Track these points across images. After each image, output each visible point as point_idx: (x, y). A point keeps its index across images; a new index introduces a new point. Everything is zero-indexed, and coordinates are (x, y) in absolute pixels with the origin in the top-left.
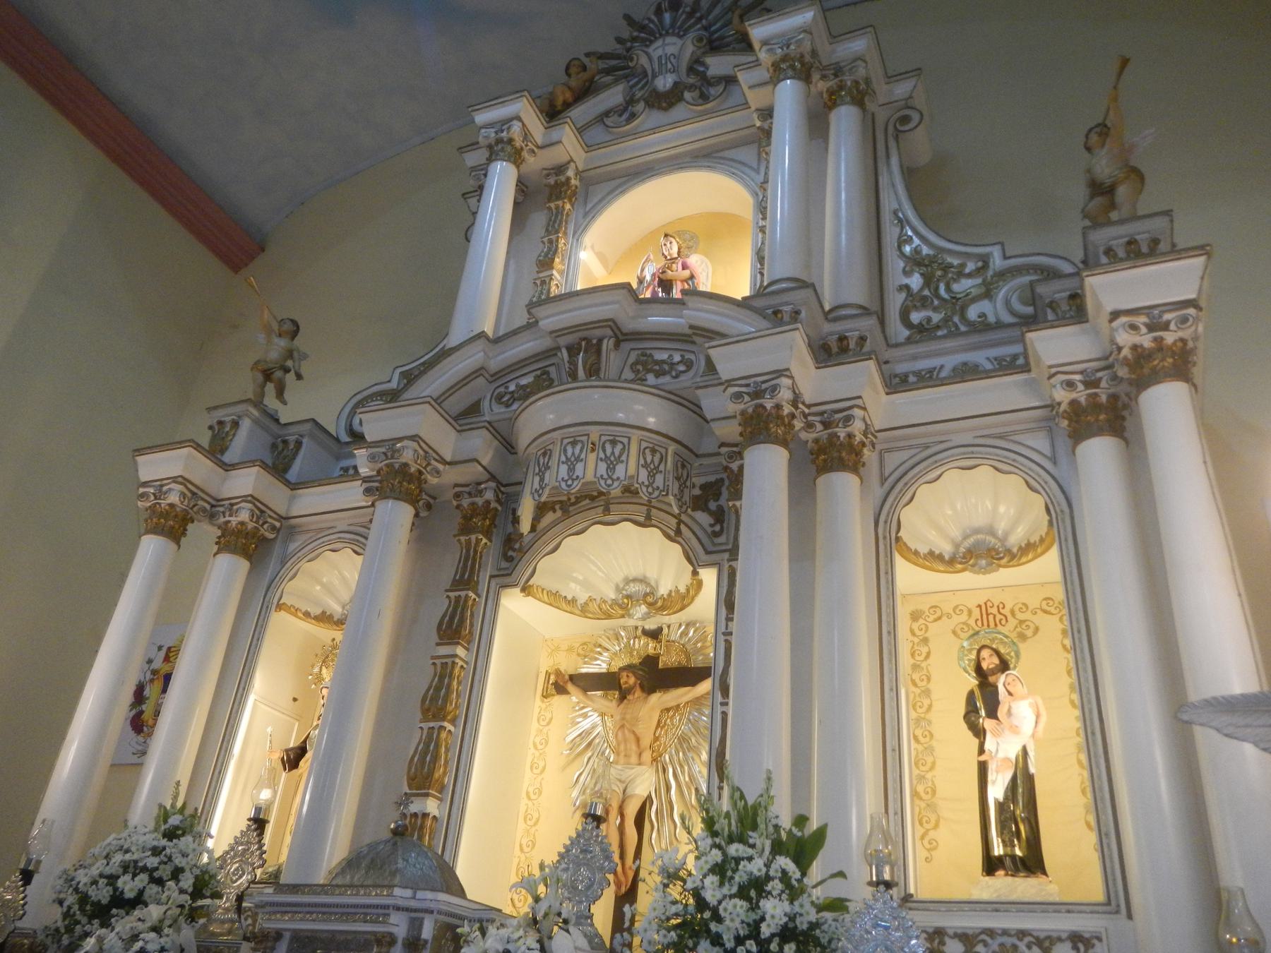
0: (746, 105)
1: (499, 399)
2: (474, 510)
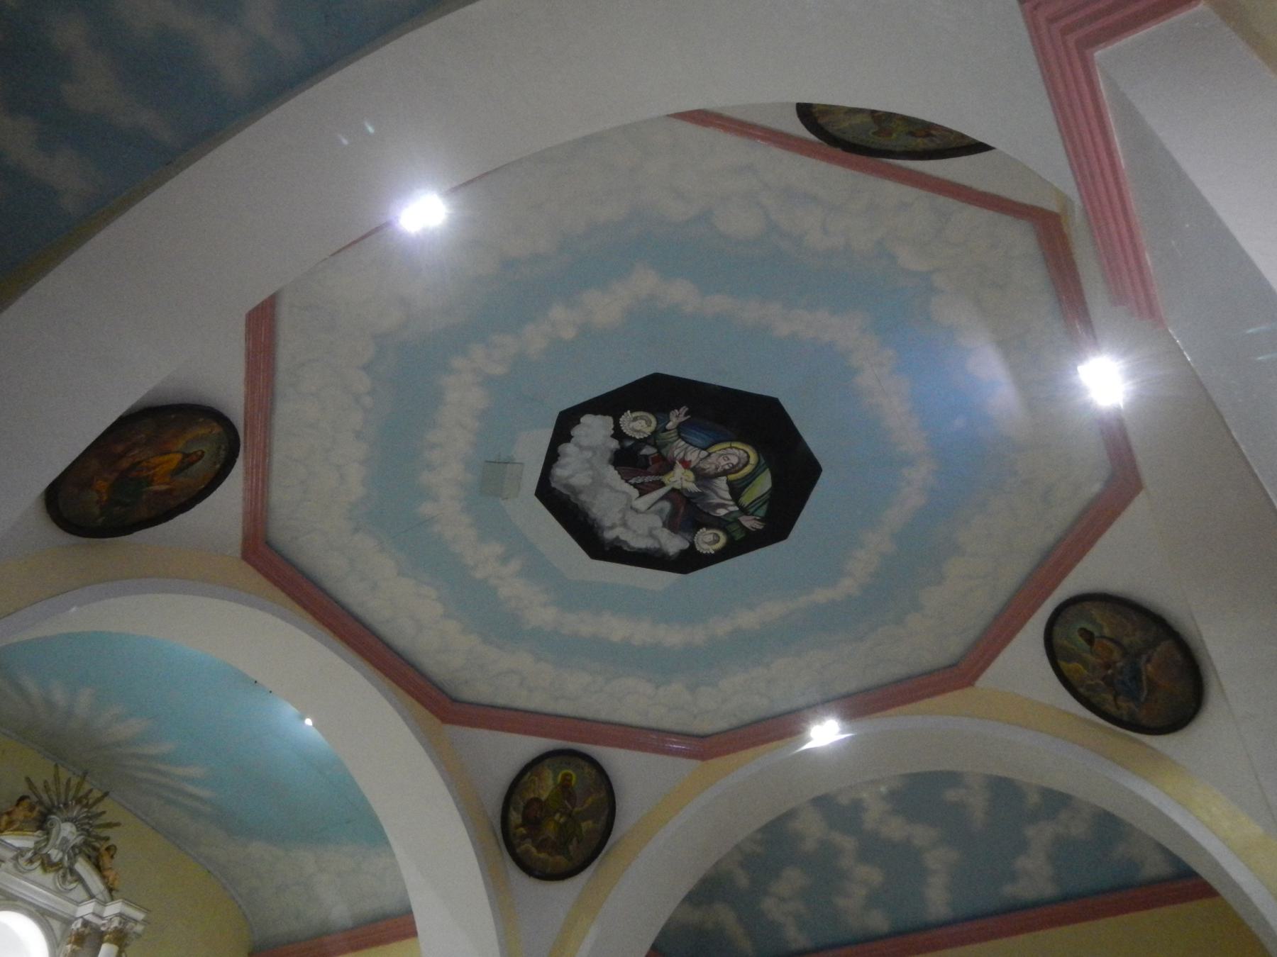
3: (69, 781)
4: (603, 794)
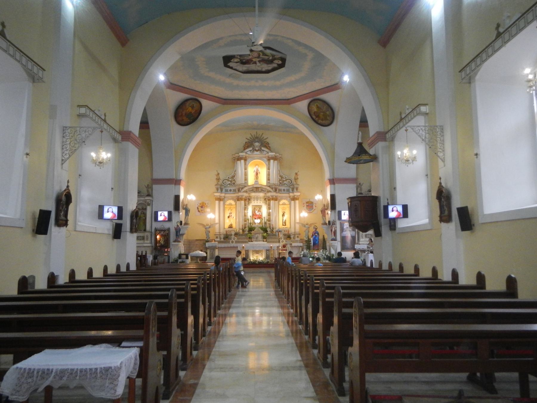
0: (266, 154)
1: (249, 191)
2: (246, 199)
3: (254, 135)
4: (326, 105)
